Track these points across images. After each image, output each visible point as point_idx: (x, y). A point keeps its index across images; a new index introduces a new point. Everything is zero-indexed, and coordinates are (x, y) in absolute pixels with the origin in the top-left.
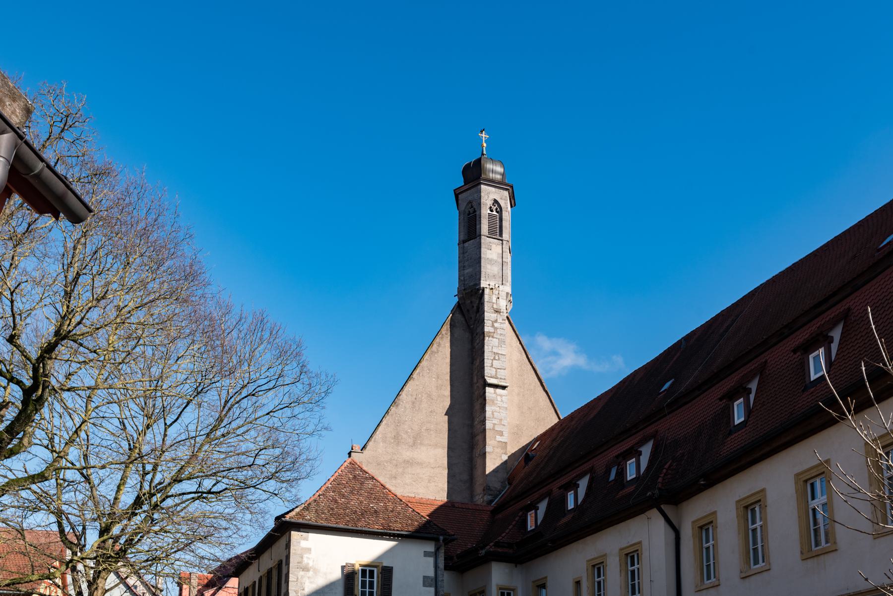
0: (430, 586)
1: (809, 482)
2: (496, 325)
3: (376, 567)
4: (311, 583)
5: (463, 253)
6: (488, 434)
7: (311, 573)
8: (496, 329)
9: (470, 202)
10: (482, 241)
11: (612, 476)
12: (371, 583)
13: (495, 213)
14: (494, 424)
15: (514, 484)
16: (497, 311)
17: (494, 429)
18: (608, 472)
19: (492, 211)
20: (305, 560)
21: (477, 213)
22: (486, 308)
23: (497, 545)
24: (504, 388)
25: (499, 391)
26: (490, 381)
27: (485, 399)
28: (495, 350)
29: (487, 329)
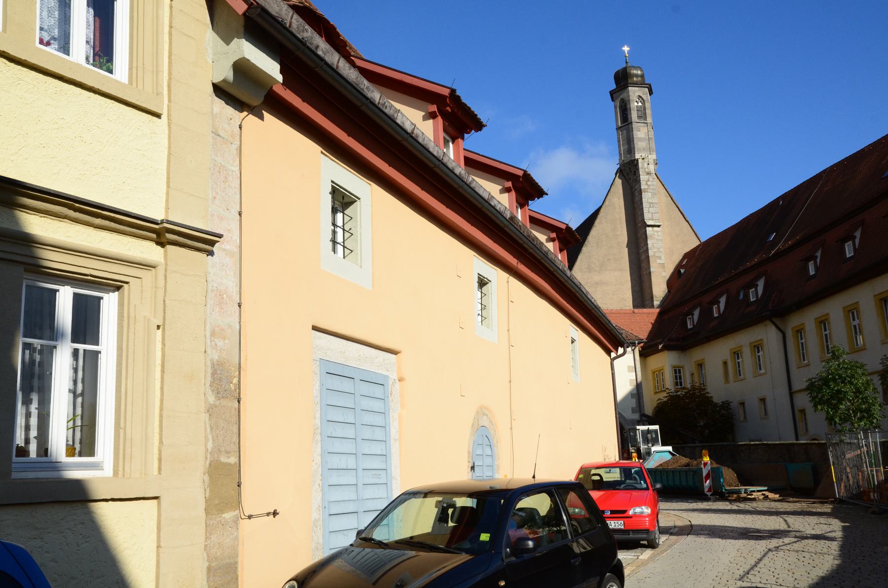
1: (852, 311)
6: (651, 260)
16: (649, 174)
24: (659, 226)
26: (649, 223)
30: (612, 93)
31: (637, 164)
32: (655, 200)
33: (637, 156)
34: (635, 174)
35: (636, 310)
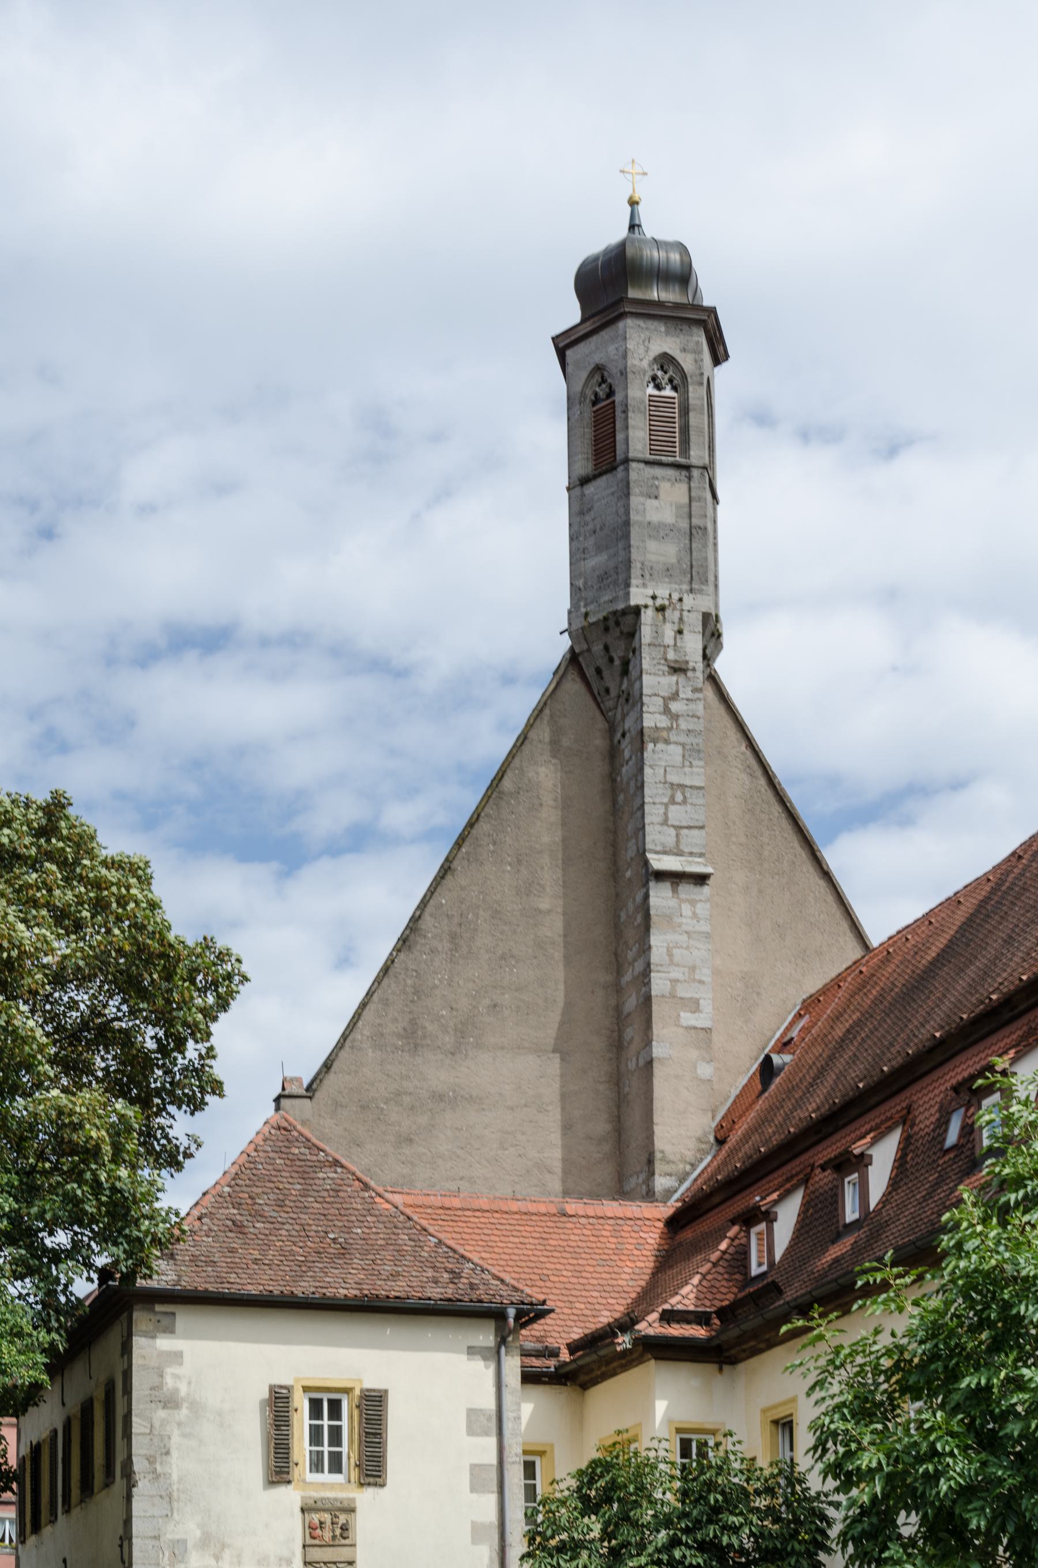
0: (487, 1434)
2: (674, 707)
3: (347, 1391)
4: (185, 1436)
5: (582, 513)
6: (658, 1010)
7: (184, 1412)
8: (675, 717)
9: (599, 369)
10: (633, 476)
11: (952, 1136)
12: (336, 1435)
13: (668, 392)
14: (675, 982)
15: (733, 1139)
16: (678, 669)
17: (673, 996)
18: (943, 1123)
19: (658, 387)
20: (169, 1382)
21: (618, 398)
25: (686, 890)
26: (660, 862)
27: (647, 916)
28: (673, 778)
29: (648, 722)
30: (564, 345)
31: (632, 634)
32: (695, 776)
33: (638, 596)
35: (572, 1207)
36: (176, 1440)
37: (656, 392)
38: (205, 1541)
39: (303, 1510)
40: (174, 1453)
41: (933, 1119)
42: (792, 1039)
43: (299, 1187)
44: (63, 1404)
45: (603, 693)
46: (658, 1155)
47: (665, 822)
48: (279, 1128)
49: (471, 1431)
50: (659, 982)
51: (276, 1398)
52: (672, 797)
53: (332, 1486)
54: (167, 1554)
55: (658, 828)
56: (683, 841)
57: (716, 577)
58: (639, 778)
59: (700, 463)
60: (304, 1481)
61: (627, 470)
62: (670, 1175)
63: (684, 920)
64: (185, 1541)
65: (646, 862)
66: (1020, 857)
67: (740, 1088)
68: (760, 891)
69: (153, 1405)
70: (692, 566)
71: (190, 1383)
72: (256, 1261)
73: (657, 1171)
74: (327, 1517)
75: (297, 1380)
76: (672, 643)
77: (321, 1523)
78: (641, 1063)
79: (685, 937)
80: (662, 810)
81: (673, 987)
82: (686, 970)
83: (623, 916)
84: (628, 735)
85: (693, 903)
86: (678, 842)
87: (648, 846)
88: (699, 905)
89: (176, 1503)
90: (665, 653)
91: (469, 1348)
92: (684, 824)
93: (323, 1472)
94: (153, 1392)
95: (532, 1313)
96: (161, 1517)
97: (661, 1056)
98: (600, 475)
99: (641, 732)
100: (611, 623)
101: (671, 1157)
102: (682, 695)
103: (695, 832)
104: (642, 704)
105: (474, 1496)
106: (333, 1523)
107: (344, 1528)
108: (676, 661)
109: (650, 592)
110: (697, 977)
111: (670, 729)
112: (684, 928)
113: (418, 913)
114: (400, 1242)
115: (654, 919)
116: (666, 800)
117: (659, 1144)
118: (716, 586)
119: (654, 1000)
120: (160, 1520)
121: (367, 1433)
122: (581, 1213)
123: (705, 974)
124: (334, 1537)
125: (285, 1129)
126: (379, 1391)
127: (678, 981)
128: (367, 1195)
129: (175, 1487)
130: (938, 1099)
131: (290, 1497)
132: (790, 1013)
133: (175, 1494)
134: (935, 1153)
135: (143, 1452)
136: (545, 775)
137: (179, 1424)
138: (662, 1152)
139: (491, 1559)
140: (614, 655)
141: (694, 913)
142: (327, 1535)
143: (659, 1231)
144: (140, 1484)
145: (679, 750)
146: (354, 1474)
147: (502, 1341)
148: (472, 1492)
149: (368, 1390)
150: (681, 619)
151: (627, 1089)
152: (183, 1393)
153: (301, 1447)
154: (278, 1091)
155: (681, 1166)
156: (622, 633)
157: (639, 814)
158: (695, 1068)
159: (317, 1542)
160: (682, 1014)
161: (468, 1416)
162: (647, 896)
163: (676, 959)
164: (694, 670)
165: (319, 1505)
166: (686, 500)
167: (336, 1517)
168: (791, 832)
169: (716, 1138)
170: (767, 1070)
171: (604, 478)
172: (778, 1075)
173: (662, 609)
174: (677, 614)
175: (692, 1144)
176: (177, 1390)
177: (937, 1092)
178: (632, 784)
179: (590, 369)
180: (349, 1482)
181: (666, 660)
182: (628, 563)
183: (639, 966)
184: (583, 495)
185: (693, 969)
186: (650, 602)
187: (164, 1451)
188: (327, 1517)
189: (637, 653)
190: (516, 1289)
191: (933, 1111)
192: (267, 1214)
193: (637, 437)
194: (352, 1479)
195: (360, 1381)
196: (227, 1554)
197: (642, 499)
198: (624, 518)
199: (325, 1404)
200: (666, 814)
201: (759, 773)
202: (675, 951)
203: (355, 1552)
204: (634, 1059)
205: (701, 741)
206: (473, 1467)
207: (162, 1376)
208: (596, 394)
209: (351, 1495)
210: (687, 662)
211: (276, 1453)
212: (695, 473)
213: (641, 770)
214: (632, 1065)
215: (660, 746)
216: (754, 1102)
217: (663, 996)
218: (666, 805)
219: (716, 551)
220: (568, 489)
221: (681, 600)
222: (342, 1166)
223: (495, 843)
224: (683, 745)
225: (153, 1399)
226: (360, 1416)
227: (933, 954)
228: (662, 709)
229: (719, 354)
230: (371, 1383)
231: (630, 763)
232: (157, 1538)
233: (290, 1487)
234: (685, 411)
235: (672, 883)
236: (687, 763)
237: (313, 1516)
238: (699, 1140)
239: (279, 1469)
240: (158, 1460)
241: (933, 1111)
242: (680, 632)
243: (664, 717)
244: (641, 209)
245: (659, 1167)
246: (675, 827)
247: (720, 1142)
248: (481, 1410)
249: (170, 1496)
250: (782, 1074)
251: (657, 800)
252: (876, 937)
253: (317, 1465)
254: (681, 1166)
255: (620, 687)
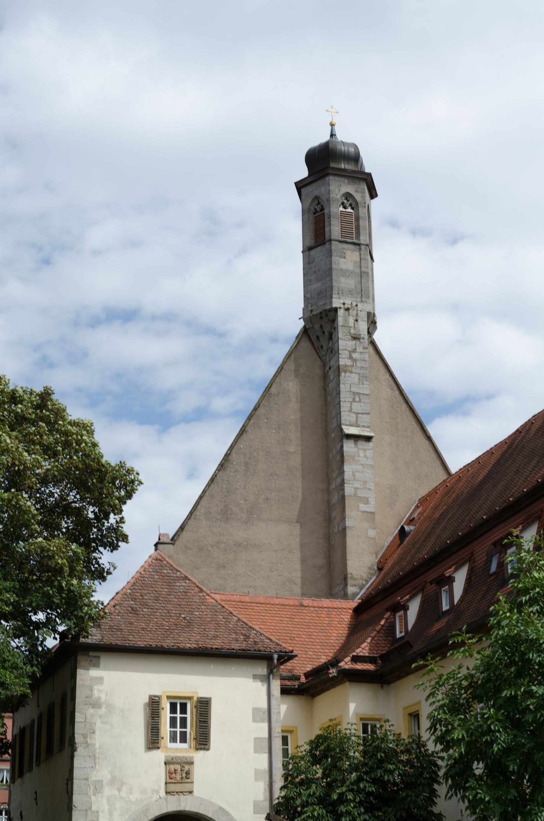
0: (263, 721)
2: (355, 356)
3: (190, 698)
4: (103, 723)
5: (309, 263)
6: (348, 503)
7: (103, 710)
8: (355, 360)
10: (333, 247)
12: (184, 722)
13: (349, 210)
16: (356, 338)
17: (355, 495)
19: (345, 207)
20: (96, 693)
21: (326, 211)
22: (340, 335)
23: (356, 659)
25: (362, 444)
27: (342, 456)
28: (354, 390)
29: (342, 362)
30: (300, 186)
31: (334, 320)
32: (365, 389)
33: (336, 303)
34: (330, 338)
35: (306, 602)
36: (98, 725)
37: (344, 210)
38: (113, 781)
39: (165, 763)
40: (97, 733)
41: (484, 559)
42: (414, 518)
43: (166, 590)
44: (38, 706)
45: (320, 348)
46: (349, 576)
47: (351, 411)
48: (157, 559)
49: (255, 720)
50: (348, 488)
51: (152, 702)
52: (354, 399)
53: (181, 750)
54: (92, 788)
55: (347, 413)
56: (359, 420)
57: (373, 296)
58: (338, 389)
59: (365, 243)
60: (166, 747)
61: (330, 244)
62: (355, 586)
63: (361, 459)
64: (102, 781)
65: (342, 430)
66: (521, 432)
67: (389, 542)
68: (397, 445)
69: (87, 706)
70: (362, 290)
71: (107, 694)
72: (143, 629)
73: (349, 584)
74: (178, 767)
75: (164, 692)
76: (352, 325)
77: (175, 770)
78: (340, 529)
79: (361, 467)
80: (349, 405)
81: (356, 492)
82: (362, 483)
83: (331, 456)
84: (332, 369)
85: (365, 450)
86: (357, 420)
87: (342, 422)
88: (368, 451)
89: (97, 760)
90: (349, 330)
91: (254, 675)
92: (360, 412)
93: (176, 742)
94: (87, 699)
95: (286, 657)
96: (89, 768)
97: (350, 525)
98: (318, 246)
99: (339, 367)
100: (324, 315)
101: (356, 577)
102: (358, 350)
103: (365, 416)
104: (339, 354)
105: (256, 755)
106: (181, 770)
107: (188, 773)
108: (355, 334)
109: (342, 302)
110: (367, 487)
111: (352, 366)
112: (361, 462)
113: (229, 452)
114: (219, 619)
115: (346, 458)
116: (351, 400)
117: (350, 570)
118: (373, 300)
119: (346, 498)
120: (89, 769)
121: (200, 721)
122: (311, 605)
123: (371, 485)
124: (182, 778)
125: (160, 560)
126: (207, 698)
127: (357, 488)
128: (201, 595)
129: (97, 751)
130: (486, 549)
131: (159, 756)
132: (413, 505)
133: (97, 755)
134: (485, 576)
135: (81, 732)
136: (291, 386)
137: (101, 717)
138: (351, 574)
139: (265, 789)
140: (325, 330)
141: (365, 455)
142: (178, 777)
143: (350, 614)
144: (78, 749)
145: (357, 376)
146: (193, 743)
147: (271, 672)
148: (255, 753)
149: (201, 698)
150: (357, 314)
151: (333, 542)
152: (103, 700)
153: (166, 729)
154: (157, 540)
155: (361, 581)
156: (329, 320)
157: (338, 406)
158: (367, 532)
159: (173, 781)
160: (360, 505)
161: (253, 712)
162: (342, 446)
163: (357, 478)
164: (363, 338)
165: (174, 760)
166: (358, 259)
167: (183, 767)
168: (411, 417)
169: (378, 567)
170: (402, 533)
171: (320, 247)
172: (407, 536)
173: (347, 309)
174: (355, 312)
175: (366, 570)
176: (100, 698)
177: (485, 545)
178: (334, 392)
179: (312, 198)
180: (191, 747)
181: (350, 333)
182: (331, 287)
183: (339, 481)
184: (310, 255)
185: (365, 482)
186: (342, 306)
187: (92, 731)
188: (178, 767)
189: (336, 330)
190: (278, 644)
191: (484, 555)
192: (150, 604)
193: (335, 230)
194: (192, 746)
195: (197, 693)
196: (124, 788)
197: (337, 258)
198: (329, 266)
199: (178, 705)
200: (351, 407)
201: (395, 388)
202: (356, 474)
203: (193, 786)
204: (337, 527)
205: (367, 372)
206: (256, 739)
207: (92, 690)
208: (315, 209)
209: (191, 755)
210: (360, 335)
211: (152, 732)
212: (363, 247)
213: (339, 385)
214: (336, 530)
215: (348, 374)
216: (396, 550)
217: (351, 496)
218: (351, 403)
219: (373, 283)
220: (303, 252)
221: (357, 305)
222: (189, 580)
223: (267, 419)
224: (359, 374)
225: (87, 703)
226: (197, 712)
227: (481, 477)
228: (348, 357)
229: (373, 194)
230: (203, 694)
231: (333, 382)
232: (87, 779)
233: (159, 751)
234: (357, 219)
235: (354, 440)
236: (361, 383)
237: (171, 766)
238: (370, 568)
239: (153, 741)
240: (89, 736)
241: (484, 555)
242: (357, 320)
243: (349, 360)
244: (336, 128)
245: (350, 582)
246: (356, 413)
247: (380, 569)
248: (260, 708)
249: (95, 756)
250: (410, 536)
251: (347, 400)
252: (454, 468)
253: (173, 739)
254: (361, 581)
255: (328, 345)
